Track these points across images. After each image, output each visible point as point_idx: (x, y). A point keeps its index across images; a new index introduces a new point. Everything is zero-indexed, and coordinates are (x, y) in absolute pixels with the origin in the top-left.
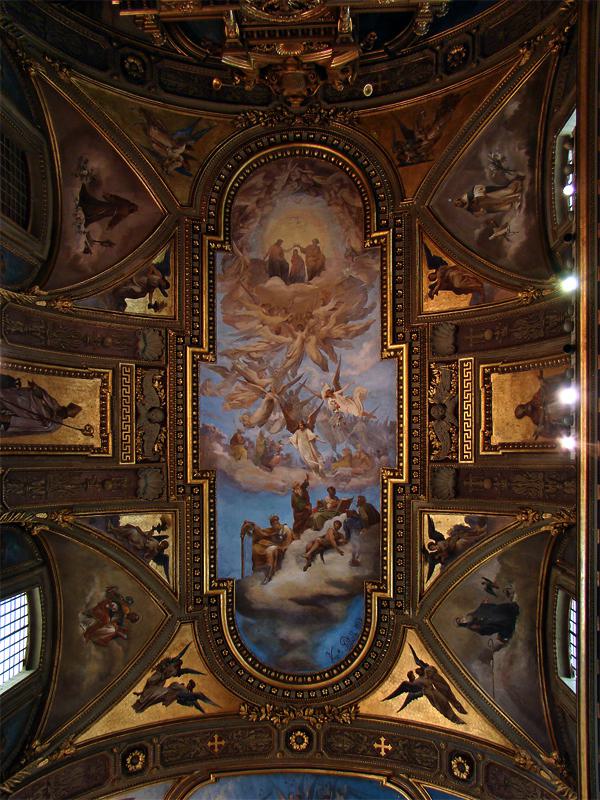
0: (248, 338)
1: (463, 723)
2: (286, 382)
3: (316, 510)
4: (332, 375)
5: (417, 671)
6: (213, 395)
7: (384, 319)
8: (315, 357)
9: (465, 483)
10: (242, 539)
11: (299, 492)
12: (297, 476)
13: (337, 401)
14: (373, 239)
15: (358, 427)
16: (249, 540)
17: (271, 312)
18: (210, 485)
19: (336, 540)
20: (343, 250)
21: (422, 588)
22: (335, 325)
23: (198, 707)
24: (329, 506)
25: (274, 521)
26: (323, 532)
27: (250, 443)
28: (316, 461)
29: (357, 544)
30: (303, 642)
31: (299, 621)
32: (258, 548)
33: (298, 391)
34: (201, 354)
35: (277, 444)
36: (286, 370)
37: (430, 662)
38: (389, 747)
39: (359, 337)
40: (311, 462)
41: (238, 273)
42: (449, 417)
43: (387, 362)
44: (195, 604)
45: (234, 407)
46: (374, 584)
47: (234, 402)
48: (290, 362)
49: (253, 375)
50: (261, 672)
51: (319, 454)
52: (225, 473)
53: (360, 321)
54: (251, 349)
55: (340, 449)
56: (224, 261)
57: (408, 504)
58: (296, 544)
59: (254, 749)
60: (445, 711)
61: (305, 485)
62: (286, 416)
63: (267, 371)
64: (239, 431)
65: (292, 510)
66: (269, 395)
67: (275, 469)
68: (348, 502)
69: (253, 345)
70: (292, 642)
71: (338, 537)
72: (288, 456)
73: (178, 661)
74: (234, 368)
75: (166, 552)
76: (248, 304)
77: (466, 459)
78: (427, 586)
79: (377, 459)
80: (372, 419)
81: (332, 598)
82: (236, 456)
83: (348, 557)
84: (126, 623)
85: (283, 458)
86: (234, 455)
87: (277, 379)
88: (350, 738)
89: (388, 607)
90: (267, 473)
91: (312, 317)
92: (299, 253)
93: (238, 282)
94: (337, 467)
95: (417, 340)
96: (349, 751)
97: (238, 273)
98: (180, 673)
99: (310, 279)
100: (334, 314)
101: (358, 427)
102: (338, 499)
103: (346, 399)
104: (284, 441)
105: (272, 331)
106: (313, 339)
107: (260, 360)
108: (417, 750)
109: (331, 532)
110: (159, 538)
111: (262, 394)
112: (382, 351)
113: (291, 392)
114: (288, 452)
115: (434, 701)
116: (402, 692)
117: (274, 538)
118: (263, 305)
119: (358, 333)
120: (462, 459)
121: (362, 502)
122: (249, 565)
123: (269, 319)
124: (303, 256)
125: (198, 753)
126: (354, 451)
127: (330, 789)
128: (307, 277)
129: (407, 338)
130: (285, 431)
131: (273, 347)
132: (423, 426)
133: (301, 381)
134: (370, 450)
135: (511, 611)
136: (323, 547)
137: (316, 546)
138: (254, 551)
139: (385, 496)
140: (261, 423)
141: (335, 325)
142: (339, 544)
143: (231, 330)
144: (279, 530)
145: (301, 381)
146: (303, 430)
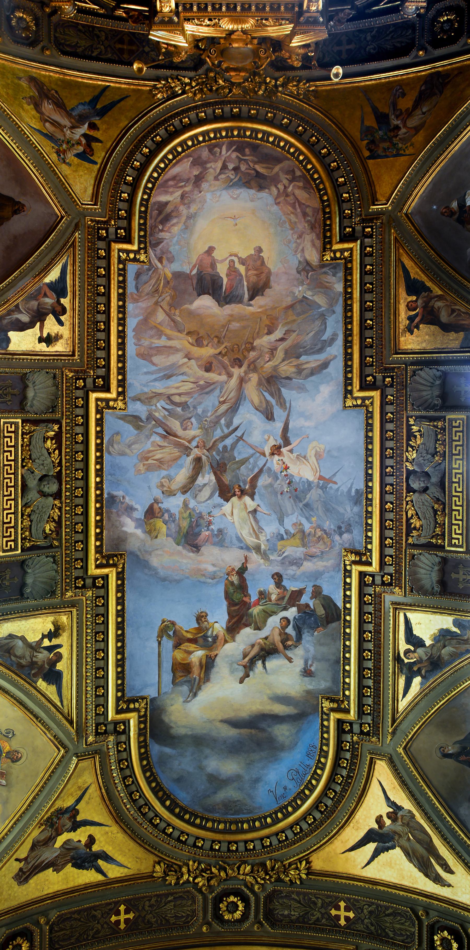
0: (168, 377)
1: (449, 885)
2: (218, 433)
3: (257, 603)
4: (279, 425)
5: (389, 815)
6: (123, 454)
7: (348, 357)
8: (256, 401)
9: (453, 576)
10: (160, 643)
11: (235, 579)
13: (285, 459)
14: (335, 252)
15: (313, 495)
16: (168, 644)
17: (199, 343)
18: (118, 573)
19: (283, 642)
20: (294, 262)
21: (395, 710)
22: (283, 360)
23: (99, 870)
24: (274, 597)
25: (201, 618)
26: (265, 632)
27: (171, 515)
28: (258, 538)
29: (312, 649)
30: (238, 778)
32: (179, 655)
33: (234, 446)
34: (107, 401)
35: (206, 517)
36: (219, 418)
37: (406, 804)
38: (351, 915)
39: (313, 378)
40: (251, 540)
41: (157, 291)
42: (434, 491)
43: (353, 413)
44: (97, 734)
45: (149, 468)
46: (332, 701)
47: (150, 461)
48: (224, 407)
49: (175, 425)
50: (182, 819)
51: (260, 528)
52: (137, 556)
53: (316, 357)
54: (174, 391)
55: (289, 523)
56: (138, 275)
57: (378, 598)
59: (172, 921)
61: (242, 571)
62: (219, 480)
63: (193, 420)
64: (156, 501)
65: (224, 604)
66: (196, 452)
67: (203, 549)
68: (300, 593)
70: (223, 777)
71: (285, 638)
72: (220, 531)
73: (73, 811)
74: (150, 417)
75: (60, 666)
76: (168, 332)
77: (455, 546)
78: (403, 704)
79: (337, 538)
80: (331, 485)
81: (277, 719)
82: (152, 533)
83: (299, 664)
85: (213, 535)
86: (149, 532)
87: (207, 431)
88: (299, 902)
89: (351, 731)
90: (191, 554)
91: (253, 349)
92: (237, 265)
93: (156, 303)
94: (285, 547)
95: (392, 386)
96: (297, 920)
97: (157, 291)
98: (76, 826)
99: (251, 298)
100: (282, 347)
101: (313, 495)
102: (285, 589)
103: (298, 457)
104: (216, 513)
105: (199, 366)
106: (254, 378)
107: (184, 406)
108: (386, 918)
109: (277, 632)
110: (50, 649)
111: (187, 450)
112: (345, 397)
113: (225, 447)
114: (222, 526)
115: (409, 855)
116: (368, 842)
117: (201, 641)
118: (189, 333)
119: (313, 372)
120: (450, 545)
121: (317, 592)
122: (167, 677)
123: (197, 351)
124: (242, 269)
125: (98, 932)
126: (307, 527)
128: (246, 296)
129: (378, 383)
130: (217, 499)
131: (202, 388)
132: (399, 498)
133: (238, 433)
134: (329, 525)
137: (256, 650)
138: (174, 659)
139: (347, 586)
140: (185, 490)
141: (283, 360)
142: (286, 647)
143: (145, 366)
144: (208, 630)
145: (238, 433)
146: (240, 497)
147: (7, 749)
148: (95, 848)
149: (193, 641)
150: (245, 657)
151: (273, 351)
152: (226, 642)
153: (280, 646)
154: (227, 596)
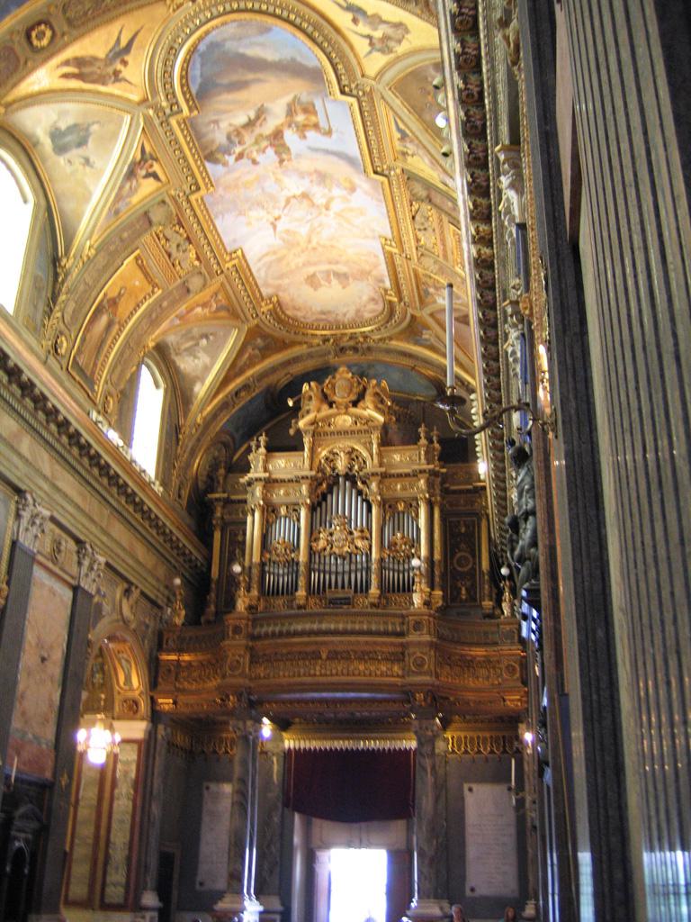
1: (58, 67)
5: (120, 72)
11: (284, 156)
16: (323, 124)
32: (313, 119)
60: (79, 62)
71: (238, 134)
119: (267, 254)
121: (225, 164)
135: (60, 149)
147: (430, 98)
150: (265, 119)
152: (282, 125)
153: (241, 130)
154: (289, 149)
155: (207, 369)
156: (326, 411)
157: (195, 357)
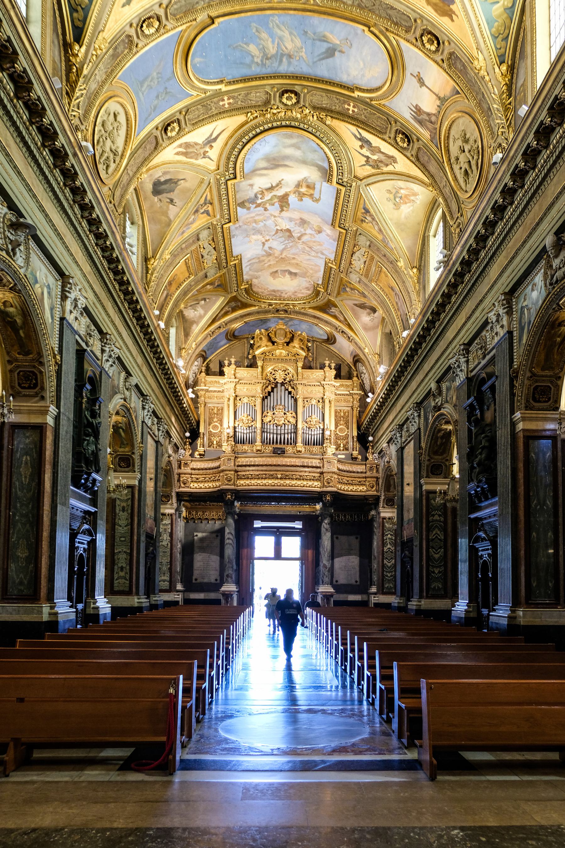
11: (285, 208)
12: (284, 214)
16: (316, 196)
17: (297, 264)
30: (285, 147)
31: (286, 157)
58: (288, 190)
61: (282, 210)
65: (290, 202)
69: (308, 257)
74: (317, 253)
81: (266, 169)
84: (394, 191)
104: (292, 226)
107: (304, 252)
111: (303, 242)
121: (249, 209)
126: (254, 225)
127: (265, 65)
130: (292, 230)
136: (271, 188)
140: (305, 234)
148: (360, 143)
149: (304, 194)
151: (269, 261)
154: (289, 205)
155: (201, 317)
156: (271, 347)
157: (195, 310)
